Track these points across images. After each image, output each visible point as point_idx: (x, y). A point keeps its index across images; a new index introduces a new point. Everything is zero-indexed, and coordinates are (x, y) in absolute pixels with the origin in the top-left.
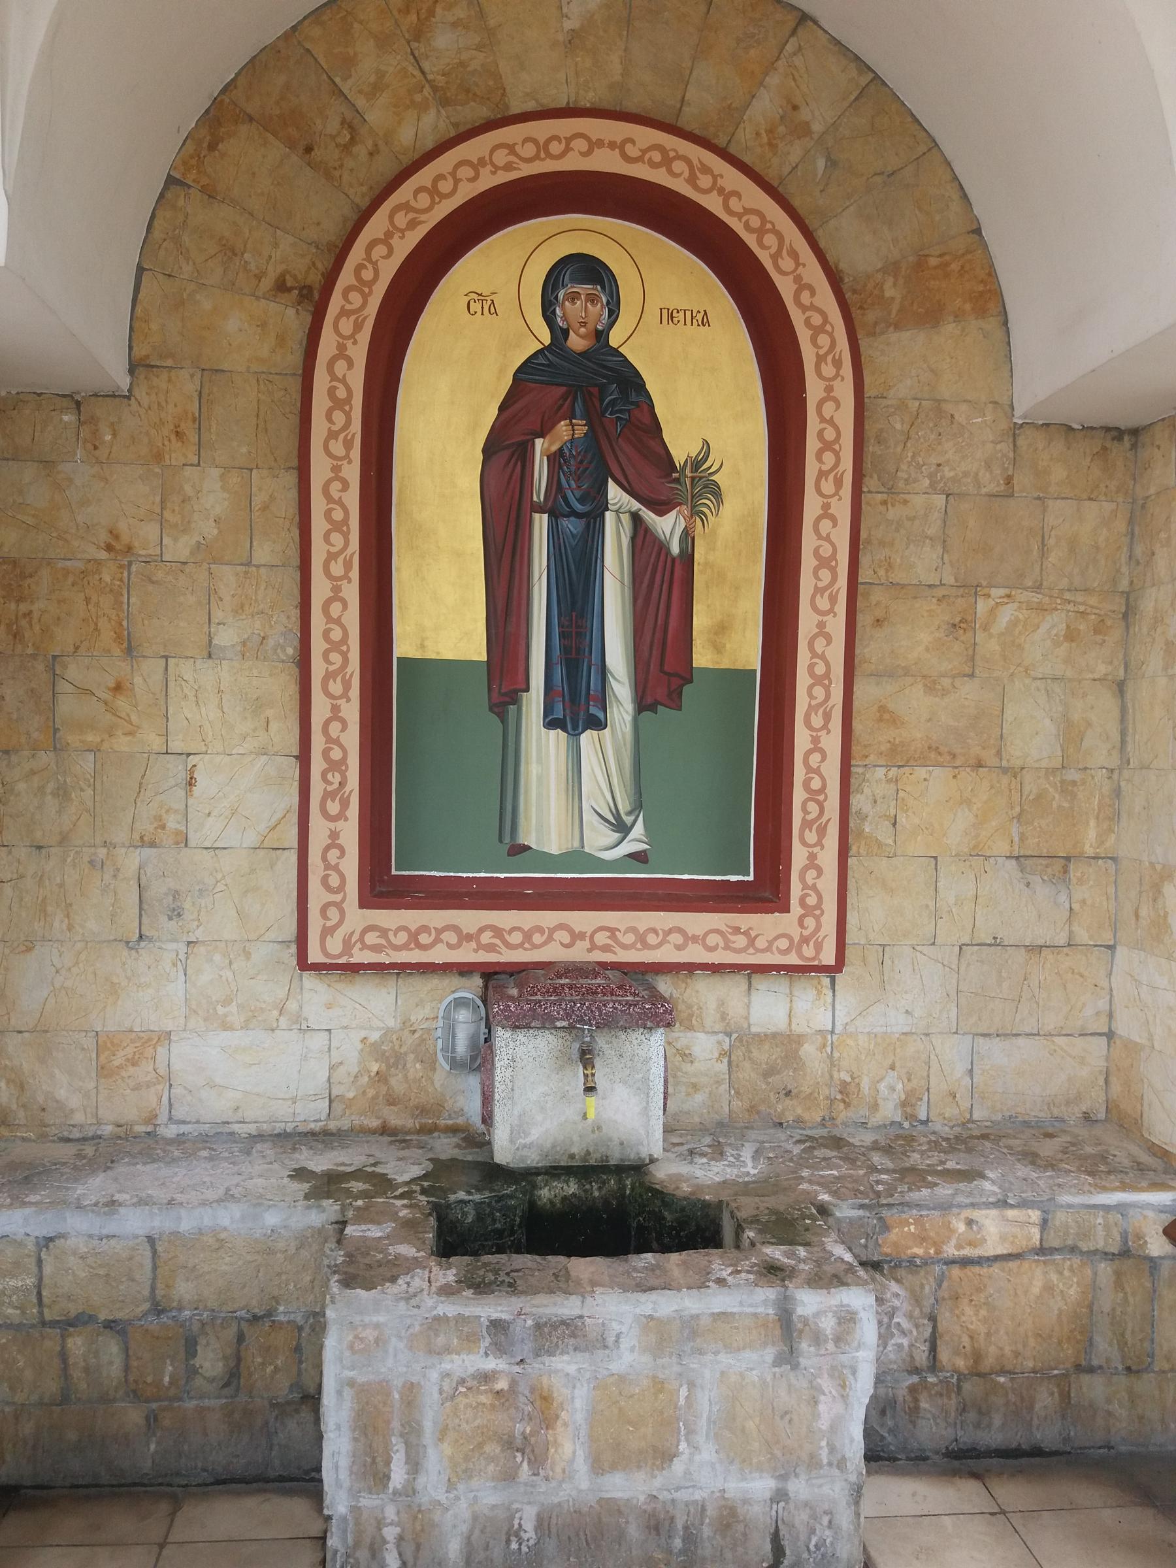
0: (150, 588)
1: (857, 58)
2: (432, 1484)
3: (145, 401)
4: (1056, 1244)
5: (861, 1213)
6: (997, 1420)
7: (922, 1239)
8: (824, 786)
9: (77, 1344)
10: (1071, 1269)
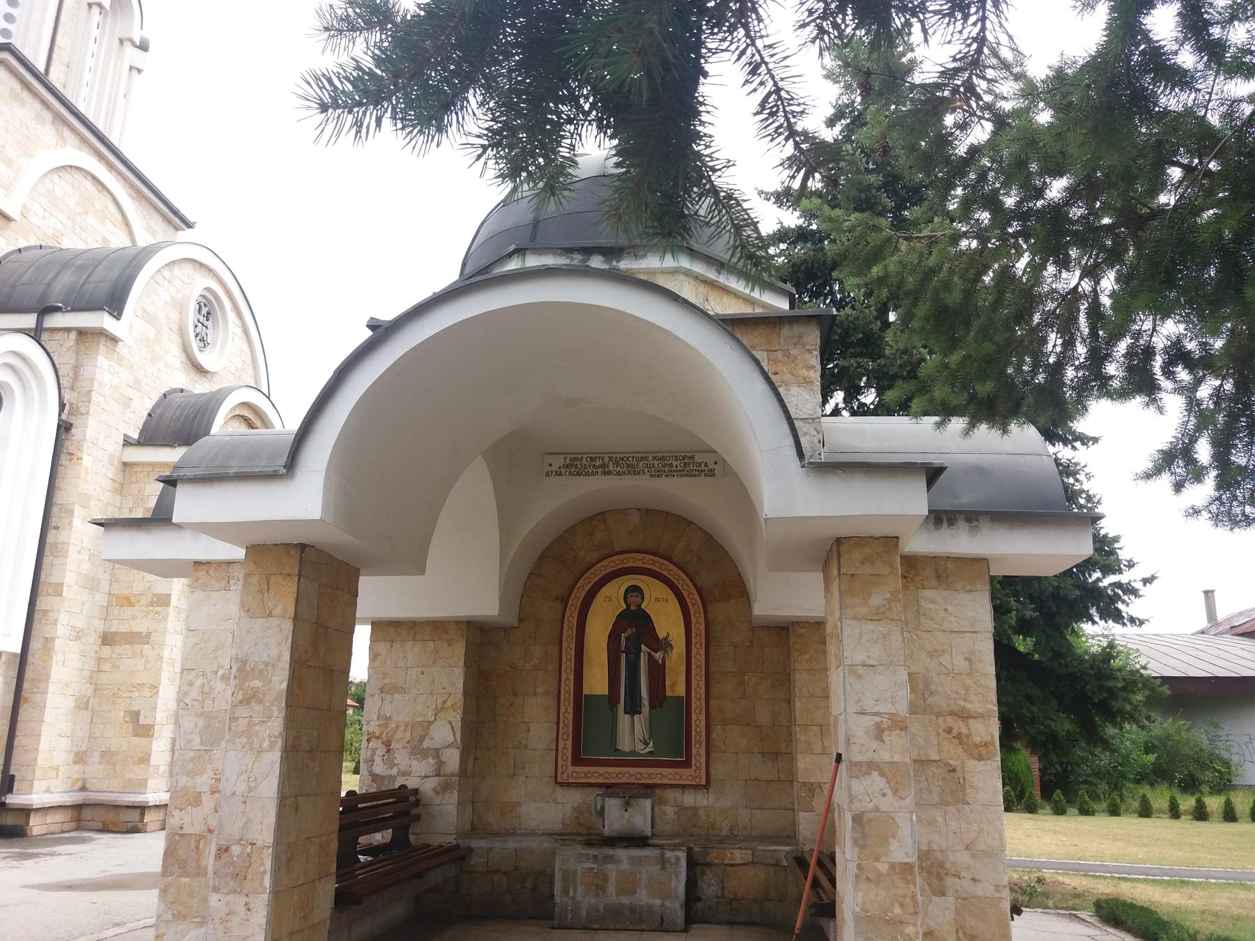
2: (579, 896)
9: (496, 877)
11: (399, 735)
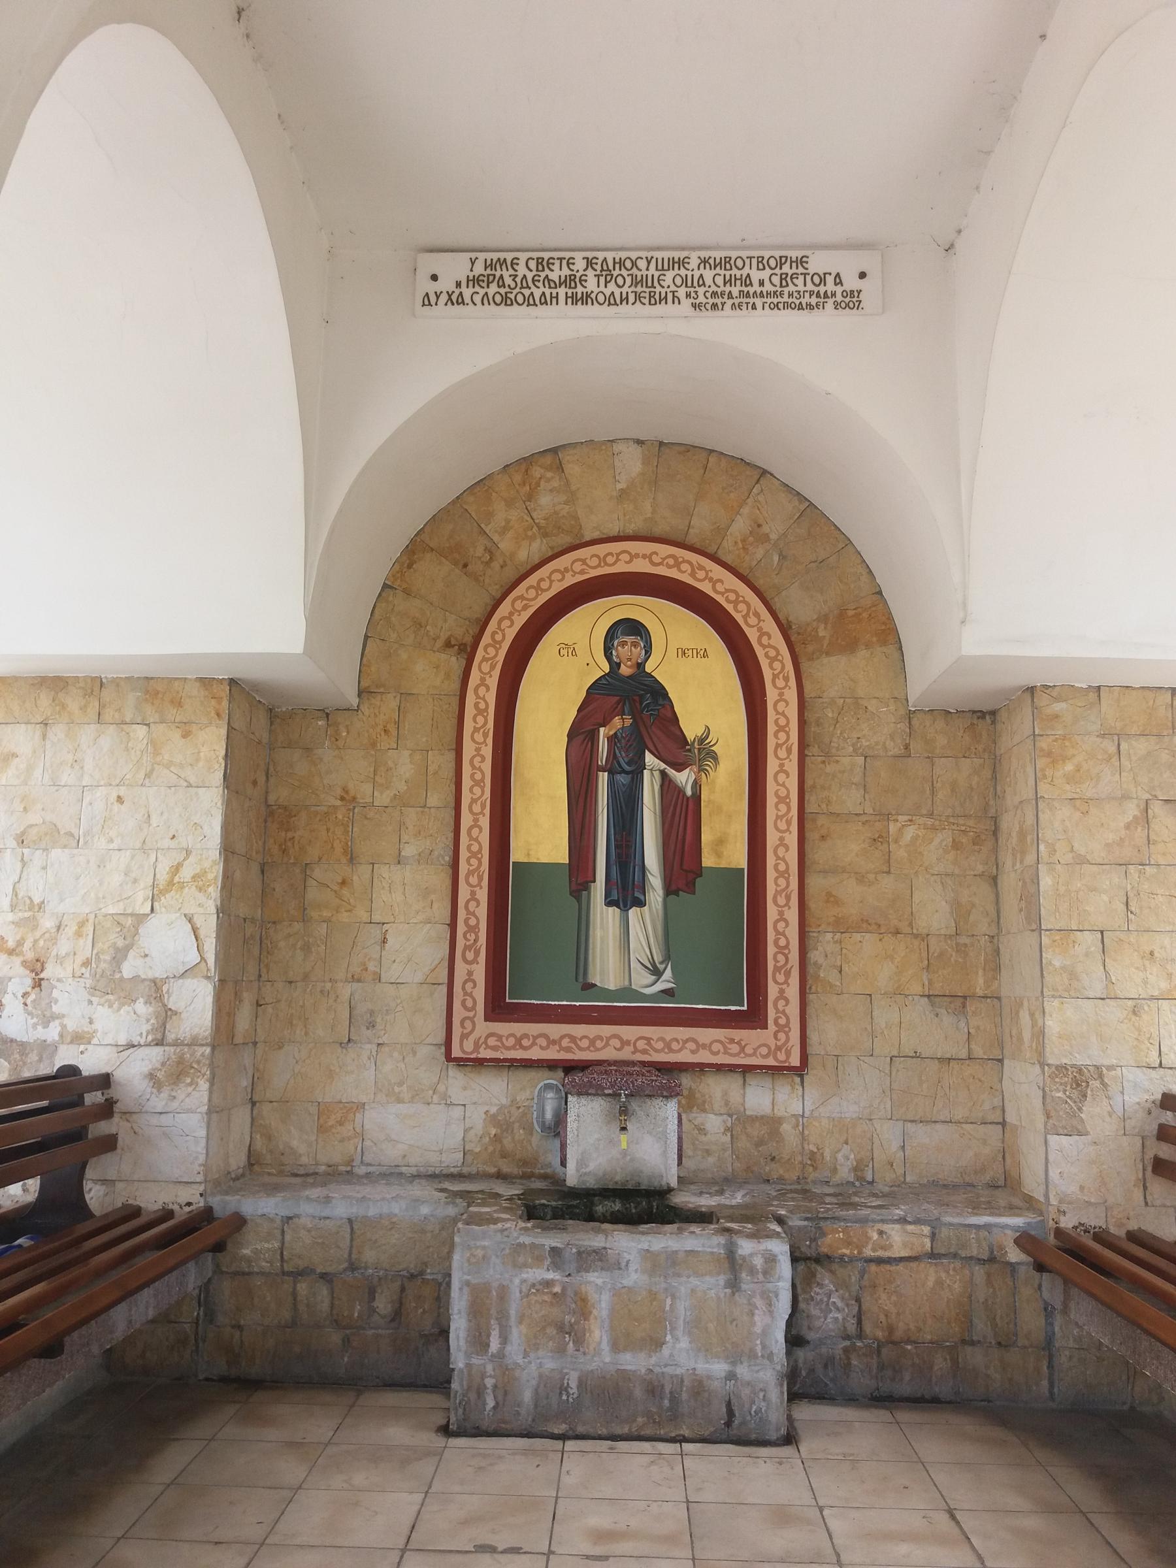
0: (366, 822)
1: (798, 493)
2: (515, 1351)
3: (367, 713)
4: (943, 1251)
5: (806, 1223)
6: (907, 1377)
7: (848, 1243)
8: (788, 943)
9: (303, 1288)
10: (954, 1269)
11: (64, 946)
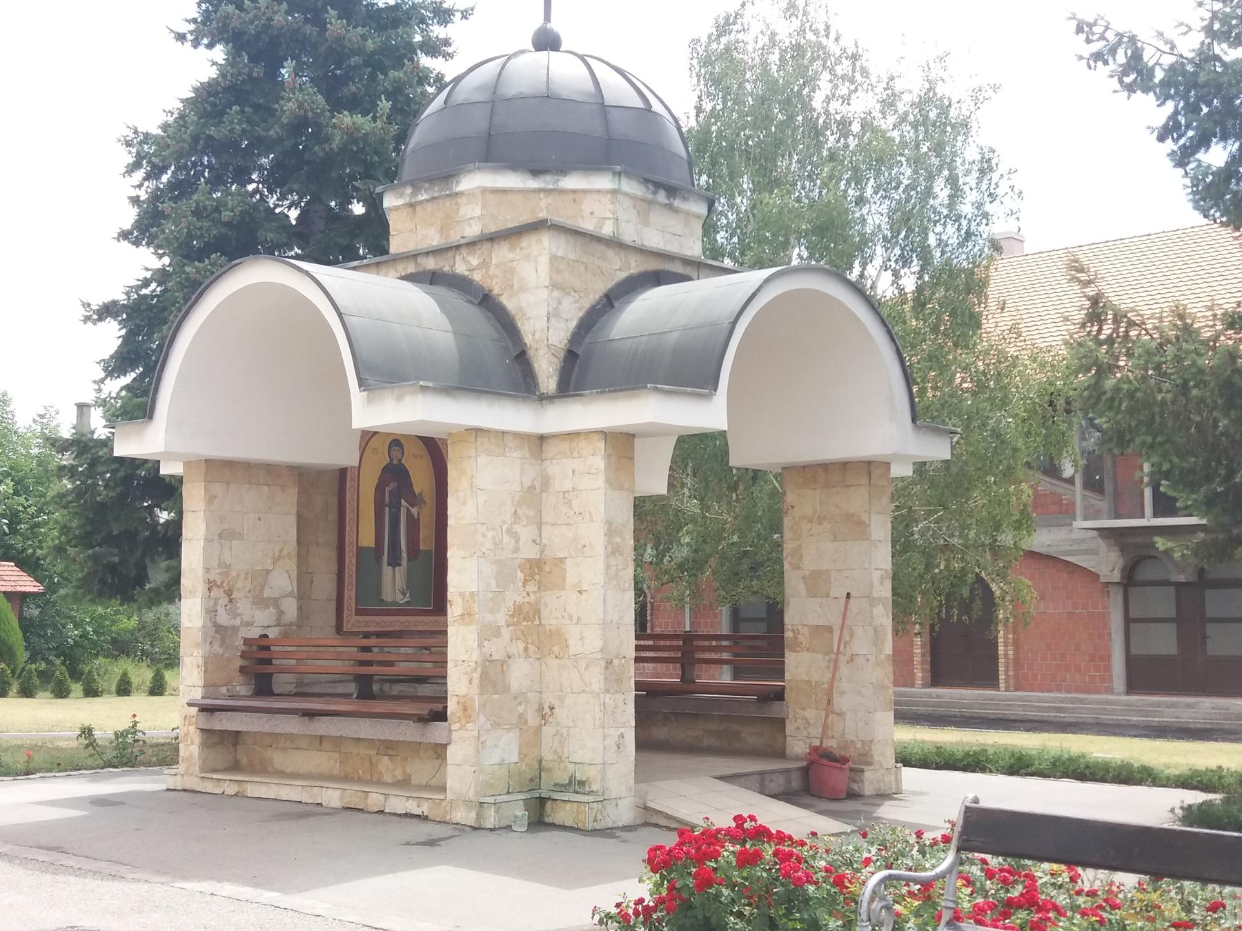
11: (240, 584)
